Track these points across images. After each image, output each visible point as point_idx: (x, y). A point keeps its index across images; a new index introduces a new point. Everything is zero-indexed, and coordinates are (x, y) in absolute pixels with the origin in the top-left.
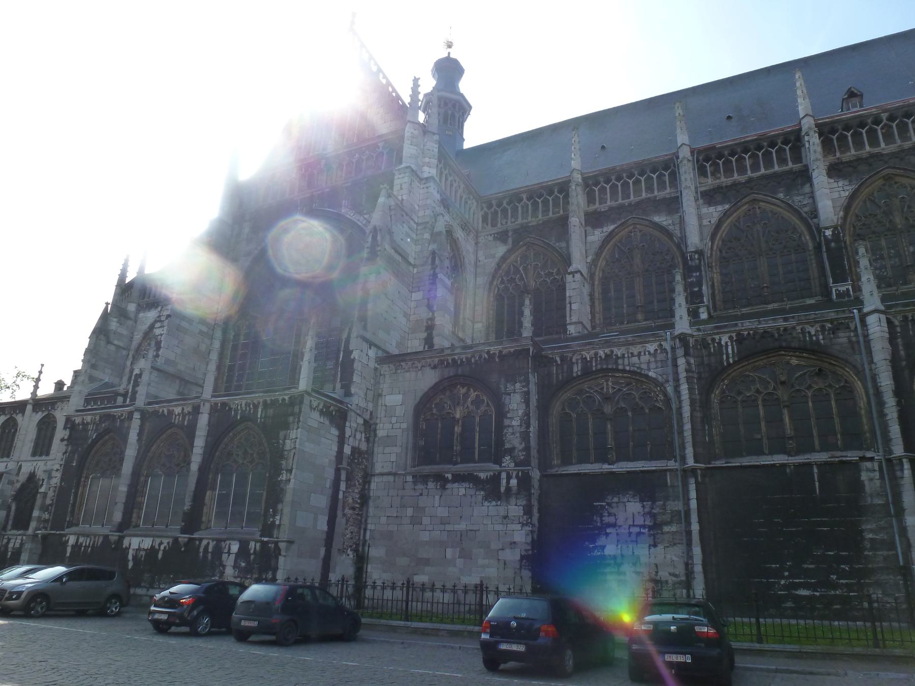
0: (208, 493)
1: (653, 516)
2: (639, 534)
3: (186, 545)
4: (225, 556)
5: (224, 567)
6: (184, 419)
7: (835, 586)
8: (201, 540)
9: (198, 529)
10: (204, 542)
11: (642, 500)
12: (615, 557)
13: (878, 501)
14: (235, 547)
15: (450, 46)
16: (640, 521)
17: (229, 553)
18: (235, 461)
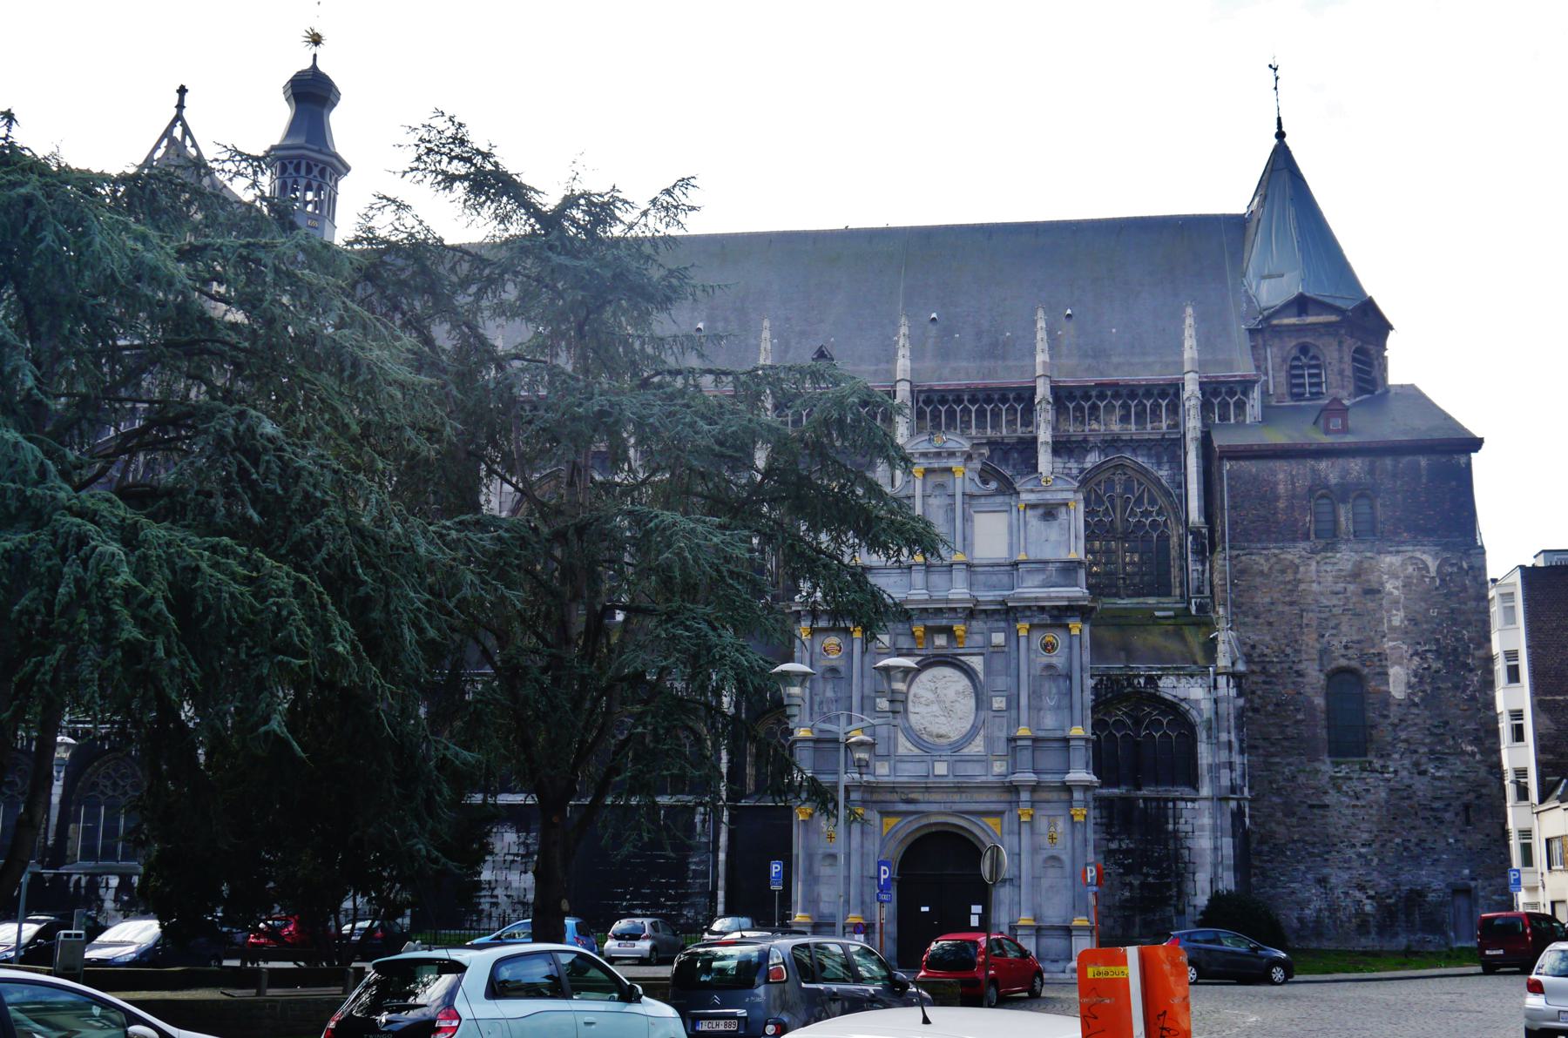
0: (72, 826)
1: (527, 846)
2: (513, 861)
3: (51, 880)
4: (102, 892)
5: (103, 901)
6: (29, 743)
7: (663, 906)
8: (69, 875)
9: (63, 863)
10: (75, 877)
11: (518, 831)
12: (489, 882)
13: (704, 840)
14: (114, 882)
15: (316, 40)
16: (514, 850)
17: (107, 887)
18: (102, 793)
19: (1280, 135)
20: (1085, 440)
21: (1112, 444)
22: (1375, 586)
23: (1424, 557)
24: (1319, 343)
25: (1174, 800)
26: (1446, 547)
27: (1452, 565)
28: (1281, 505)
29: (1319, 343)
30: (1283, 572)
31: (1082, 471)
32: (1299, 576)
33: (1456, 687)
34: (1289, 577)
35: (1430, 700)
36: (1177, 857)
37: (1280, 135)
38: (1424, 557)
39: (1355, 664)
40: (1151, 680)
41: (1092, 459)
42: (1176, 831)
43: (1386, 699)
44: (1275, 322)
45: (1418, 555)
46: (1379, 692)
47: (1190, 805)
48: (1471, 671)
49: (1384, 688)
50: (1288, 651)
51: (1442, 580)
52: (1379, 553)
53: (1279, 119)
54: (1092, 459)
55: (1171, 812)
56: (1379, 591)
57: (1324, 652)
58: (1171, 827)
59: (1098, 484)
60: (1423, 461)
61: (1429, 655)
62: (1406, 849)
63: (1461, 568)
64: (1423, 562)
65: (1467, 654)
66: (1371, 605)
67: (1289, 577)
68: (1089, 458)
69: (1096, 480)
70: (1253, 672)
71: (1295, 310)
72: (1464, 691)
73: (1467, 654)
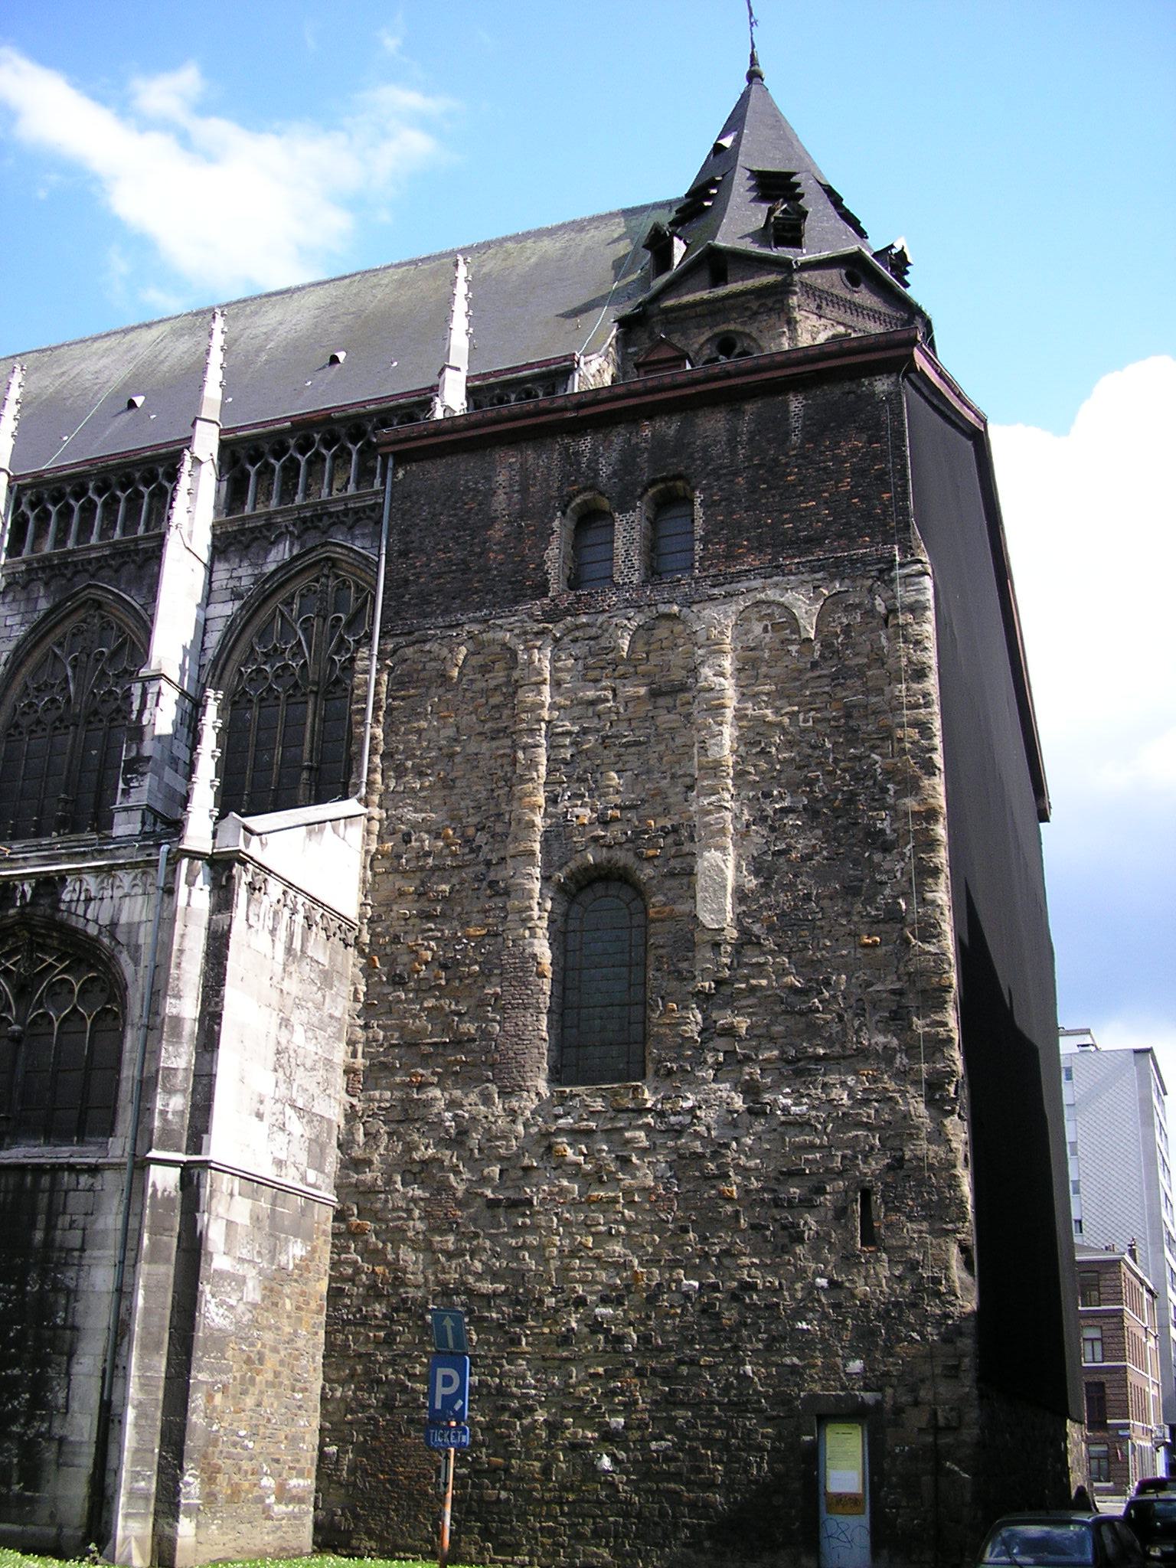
19: (754, 76)
20: (269, 525)
21: (316, 521)
22: (677, 675)
23: (788, 597)
24: (752, 329)
25: (56, 1169)
26: (836, 569)
27: (849, 609)
28: (497, 532)
29: (752, 329)
30: (485, 669)
31: (257, 579)
32: (516, 674)
33: (851, 891)
34: (498, 676)
35: (789, 924)
36: (43, 1309)
37: (754, 76)
38: (788, 597)
39: (623, 857)
40: (50, 885)
41: (280, 553)
42: (49, 1242)
43: (689, 935)
44: (670, 303)
45: (772, 594)
46: (672, 917)
47: (84, 1180)
48: (887, 848)
49: (682, 908)
50: (481, 838)
51: (826, 645)
52: (688, 603)
53: (752, 56)
54: (280, 553)
55: (43, 1199)
56: (683, 688)
57: (558, 834)
58: (39, 1236)
59: (288, 603)
60: (795, 404)
61: (789, 821)
62: (706, 1310)
63: (871, 612)
64: (786, 608)
65: (878, 802)
66: (666, 719)
67: (498, 676)
68: (272, 556)
69: (284, 594)
70: (402, 894)
71: (705, 276)
72: (870, 900)
73: (878, 802)
